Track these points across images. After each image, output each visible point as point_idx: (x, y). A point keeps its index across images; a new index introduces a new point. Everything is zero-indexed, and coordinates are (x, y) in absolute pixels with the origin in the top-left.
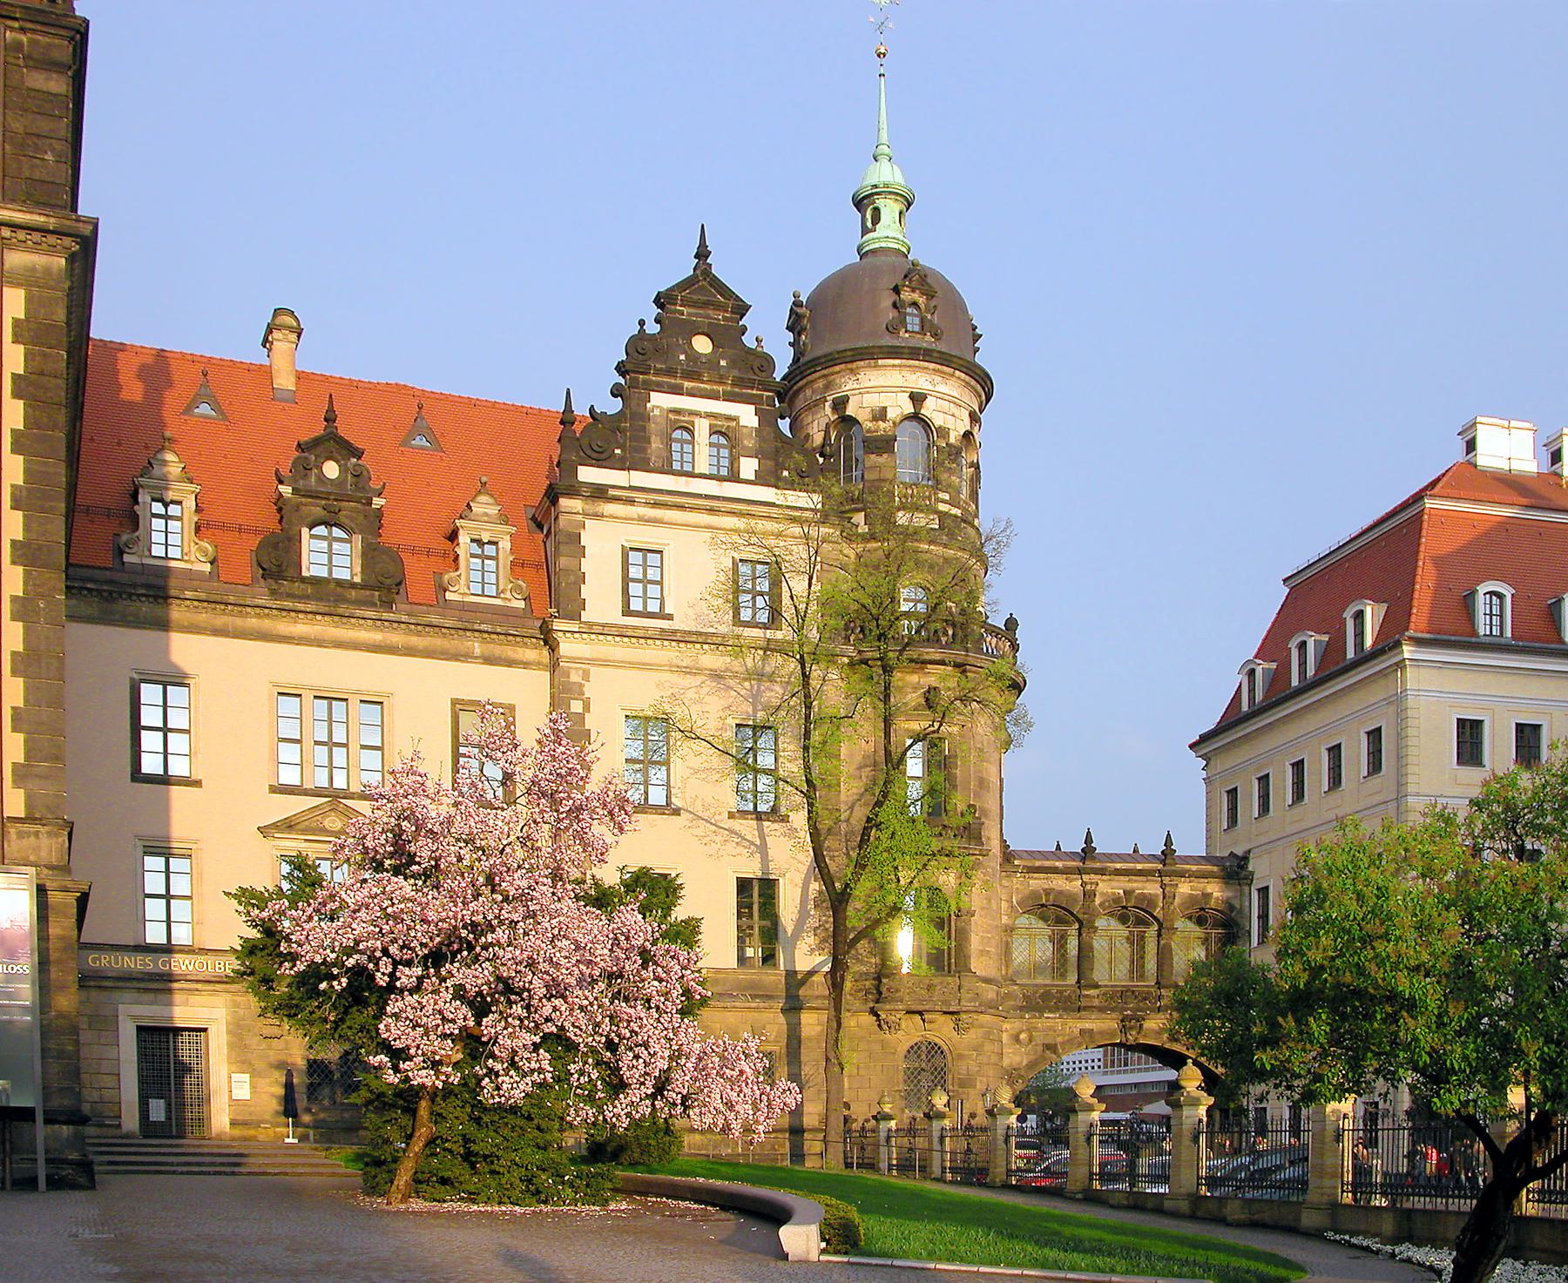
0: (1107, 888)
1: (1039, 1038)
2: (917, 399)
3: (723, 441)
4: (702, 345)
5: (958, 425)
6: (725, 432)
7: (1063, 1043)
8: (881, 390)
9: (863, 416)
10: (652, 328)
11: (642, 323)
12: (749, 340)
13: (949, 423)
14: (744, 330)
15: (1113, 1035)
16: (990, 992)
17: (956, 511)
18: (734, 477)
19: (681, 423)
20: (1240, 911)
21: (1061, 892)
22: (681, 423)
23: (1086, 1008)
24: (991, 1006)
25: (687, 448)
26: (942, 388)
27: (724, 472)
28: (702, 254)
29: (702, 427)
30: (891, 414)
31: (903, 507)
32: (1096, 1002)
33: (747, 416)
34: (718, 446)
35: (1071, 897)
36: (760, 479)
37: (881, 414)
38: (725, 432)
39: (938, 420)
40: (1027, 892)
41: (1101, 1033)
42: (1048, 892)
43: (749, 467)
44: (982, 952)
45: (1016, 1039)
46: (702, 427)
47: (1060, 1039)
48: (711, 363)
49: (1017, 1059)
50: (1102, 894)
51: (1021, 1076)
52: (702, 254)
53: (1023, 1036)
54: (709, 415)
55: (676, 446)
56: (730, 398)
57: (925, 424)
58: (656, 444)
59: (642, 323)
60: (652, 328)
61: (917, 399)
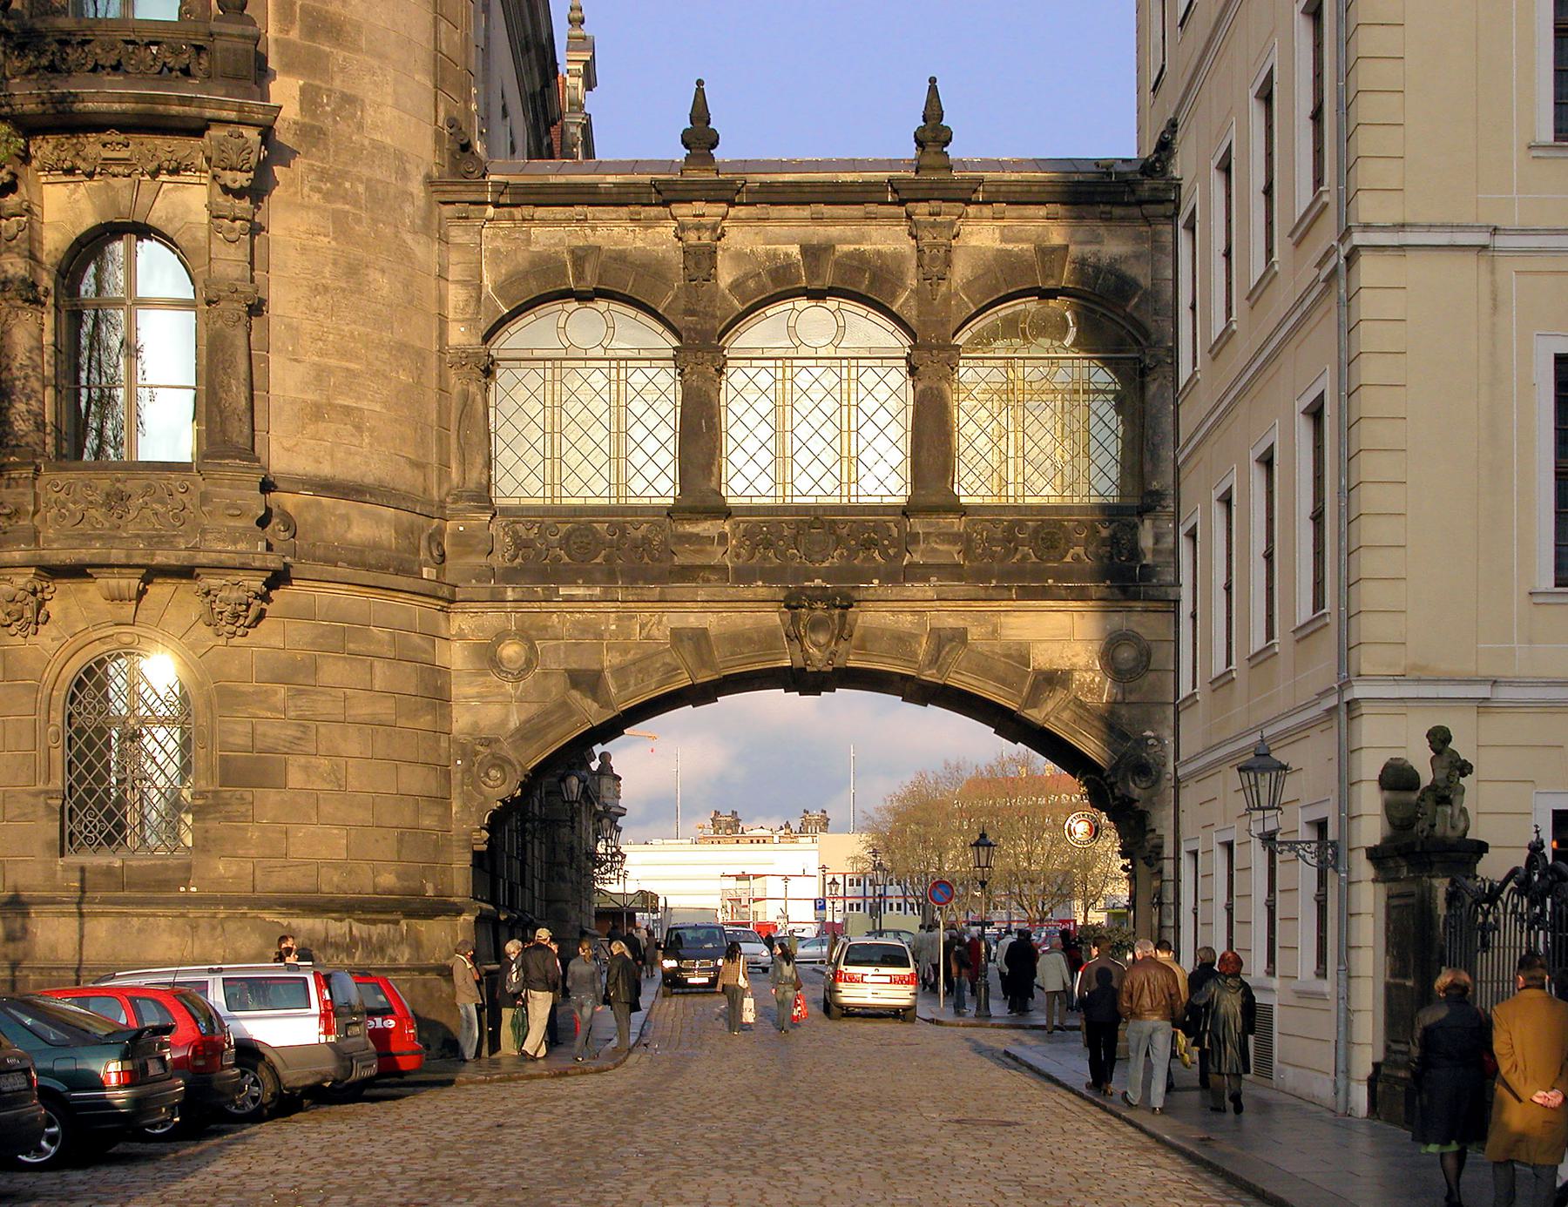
0: (750, 240)
1: (556, 659)
7: (620, 671)
15: (766, 640)
16: (367, 526)
20: (1153, 295)
21: (621, 258)
23: (687, 573)
24: (383, 568)
32: (717, 556)
35: (650, 269)
40: (522, 259)
41: (736, 639)
42: (580, 256)
44: (317, 412)
45: (487, 657)
47: (610, 660)
49: (490, 715)
50: (739, 257)
51: (500, 762)
53: (511, 651)
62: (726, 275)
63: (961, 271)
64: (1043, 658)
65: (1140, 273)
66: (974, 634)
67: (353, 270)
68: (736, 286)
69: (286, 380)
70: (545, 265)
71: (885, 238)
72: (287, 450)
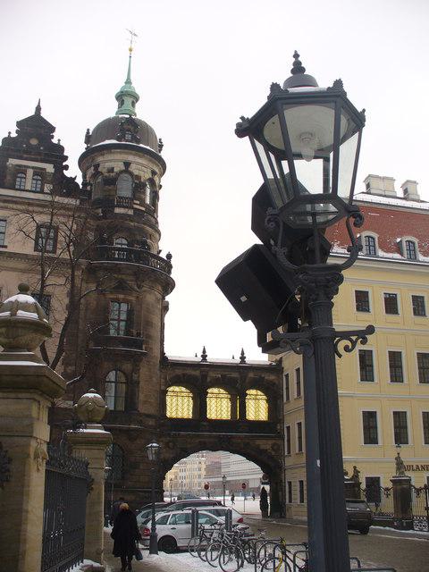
2: (127, 164)
3: (39, 178)
4: (34, 142)
5: (146, 175)
6: (39, 173)
8: (110, 161)
9: (104, 171)
10: (14, 135)
11: (10, 133)
12: (55, 141)
13: (141, 174)
14: (53, 137)
16: (151, 422)
17: (144, 209)
18: (42, 192)
19: (21, 170)
21: (190, 375)
22: (21, 170)
25: (23, 180)
26: (140, 160)
27: (38, 190)
28: (38, 109)
29: (30, 173)
30: (115, 170)
31: (119, 206)
33: (50, 168)
34: (37, 180)
36: (52, 193)
37: (111, 170)
38: (39, 173)
39: (136, 172)
42: (184, 375)
43: (47, 188)
44: (145, 402)
46: (30, 173)
48: (37, 147)
52: (38, 109)
54: (33, 168)
55: (18, 179)
56: (42, 161)
57: (131, 174)
58: (9, 178)
59: (10, 133)
60: (14, 135)
61: (127, 164)
62: (209, 380)
63: (247, 381)
64: (262, 447)
65: (277, 383)
66: (251, 443)
67: (151, 378)
68: (210, 382)
69: (141, 397)
70: (178, 376)
71: (235, 375)
72: (142, 409)
